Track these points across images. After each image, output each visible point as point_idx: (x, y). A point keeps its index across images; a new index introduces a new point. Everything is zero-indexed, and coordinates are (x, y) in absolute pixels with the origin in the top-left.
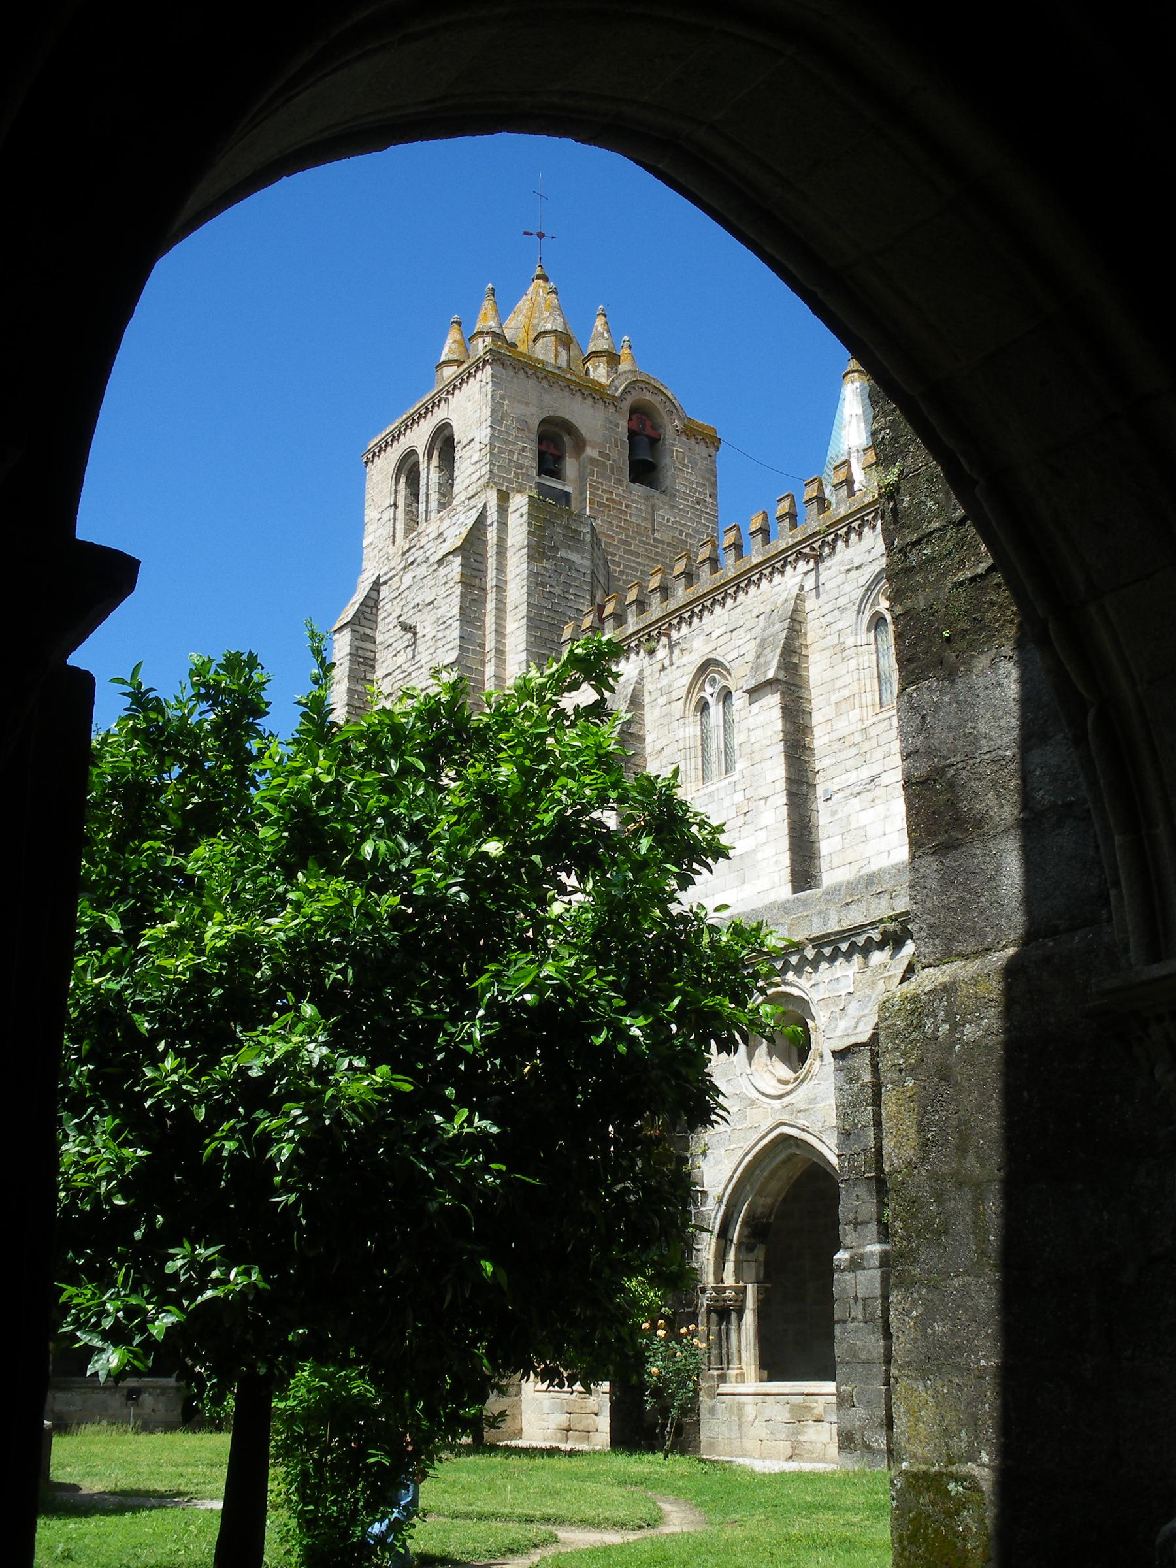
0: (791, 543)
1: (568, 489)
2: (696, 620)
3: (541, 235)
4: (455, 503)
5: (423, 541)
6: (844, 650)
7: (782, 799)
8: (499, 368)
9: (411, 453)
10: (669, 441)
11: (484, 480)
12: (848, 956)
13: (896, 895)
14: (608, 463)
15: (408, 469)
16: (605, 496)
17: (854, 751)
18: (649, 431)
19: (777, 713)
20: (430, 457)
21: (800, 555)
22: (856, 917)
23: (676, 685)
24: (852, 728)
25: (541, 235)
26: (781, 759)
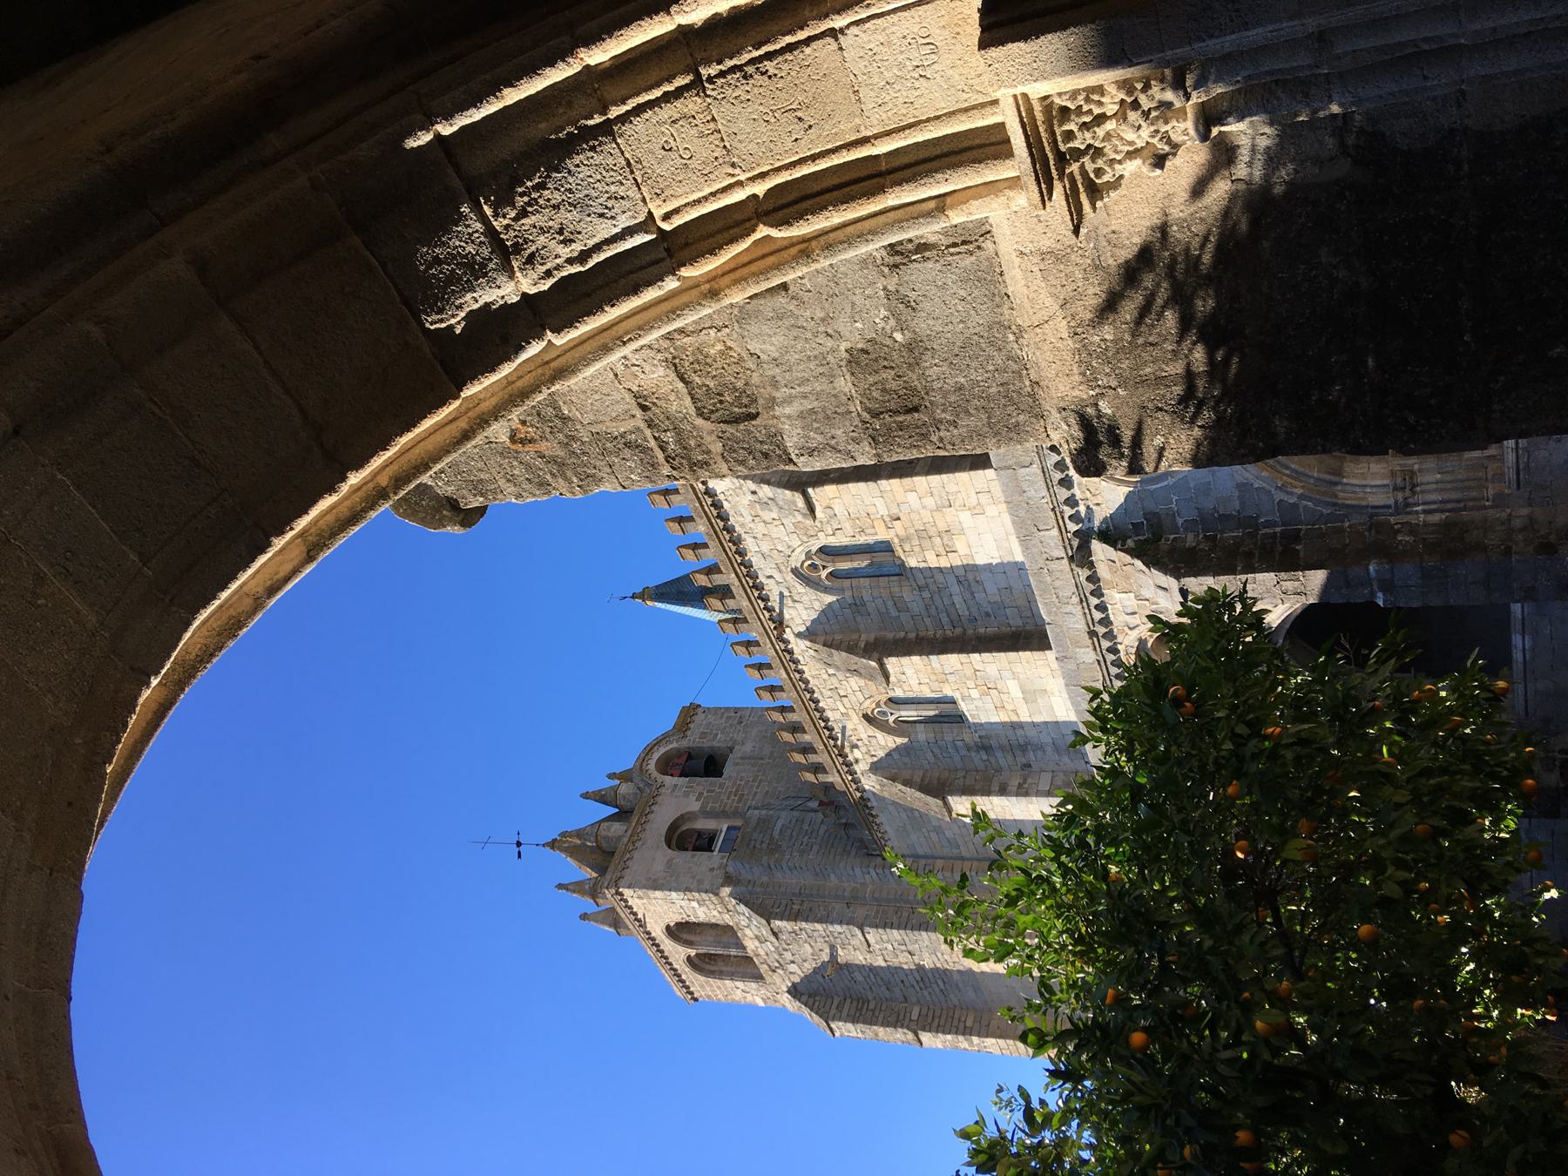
0: (770, 645)
1: (725, 829)
3: (519, 844)
4: (731, 924)
5: (762, 953)
6: (855, 604)
7: (975, 657)
8: (622, 882)
10: (691, 745)
11: (713, 898)
15: (700, 964)
16: (732, 797)
17: (936, 597)
19: (905, 660)
21: (780, 639)
23: (883, 743)
24: (917, 598)
26: (943, 657)
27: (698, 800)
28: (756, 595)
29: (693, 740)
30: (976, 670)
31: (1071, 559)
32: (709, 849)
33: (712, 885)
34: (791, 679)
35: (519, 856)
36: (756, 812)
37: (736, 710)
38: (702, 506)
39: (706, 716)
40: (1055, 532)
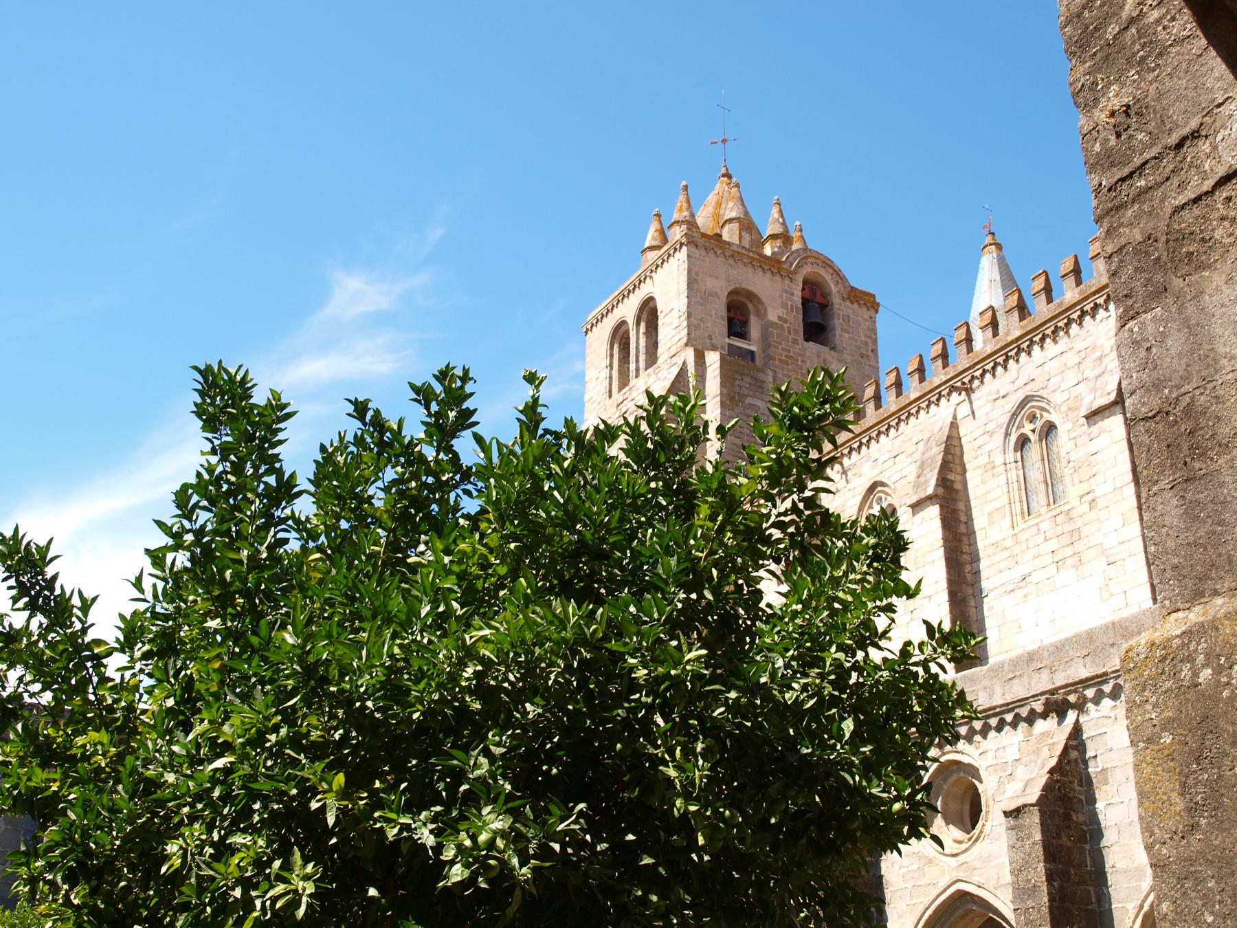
0: (944, 379)
1: (753, 348)
2: (864, 448)
4: (659, 361)
6: (994, 467)
7: (945, 596)
8: (693, 249)
9: (623, 323)
10: (836, 306)
12: (1014, 725)
13: (1055, 671)
14: (786, 325)
15: (620, 336)
16: (784, 354)
17: (1006, 554)
18: (819, 299)
19: (937, 523)
20: (638, 324)
21: (953, 389)
22: (1018, 690)
23: (848, 504)
25: (724, 141)
27: (780, 318)
28: (998, 360)
29: (841, 308)
30: (930, 597)
31: (1053, 692)
32: (732, 332)
33: (696, 340)
34: (910, 404)
35: (712, 143)
36: (770, 379)
37: (875, 351)
38: (1094, 293)
39: (866, 320)
40: (1084, 674)
